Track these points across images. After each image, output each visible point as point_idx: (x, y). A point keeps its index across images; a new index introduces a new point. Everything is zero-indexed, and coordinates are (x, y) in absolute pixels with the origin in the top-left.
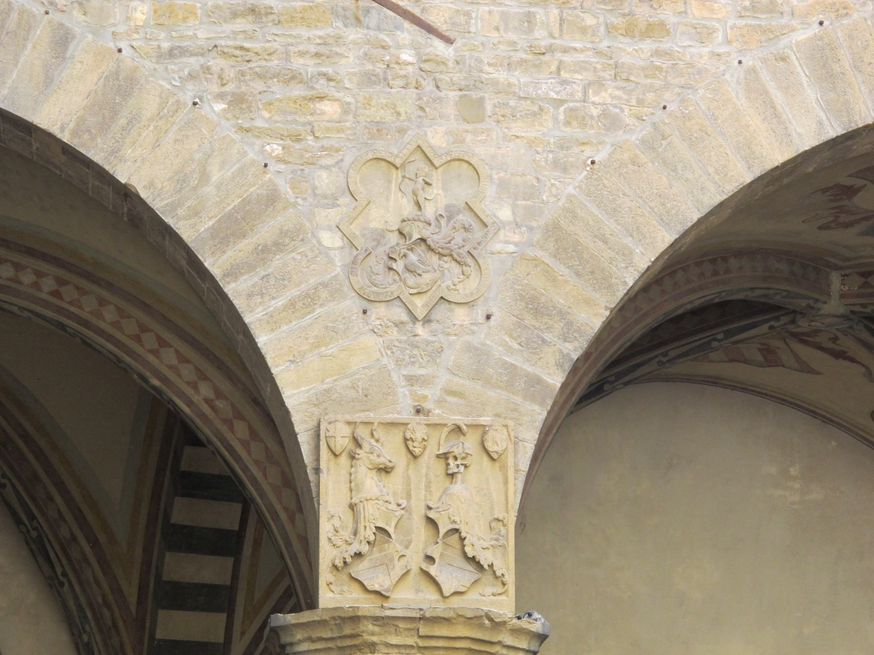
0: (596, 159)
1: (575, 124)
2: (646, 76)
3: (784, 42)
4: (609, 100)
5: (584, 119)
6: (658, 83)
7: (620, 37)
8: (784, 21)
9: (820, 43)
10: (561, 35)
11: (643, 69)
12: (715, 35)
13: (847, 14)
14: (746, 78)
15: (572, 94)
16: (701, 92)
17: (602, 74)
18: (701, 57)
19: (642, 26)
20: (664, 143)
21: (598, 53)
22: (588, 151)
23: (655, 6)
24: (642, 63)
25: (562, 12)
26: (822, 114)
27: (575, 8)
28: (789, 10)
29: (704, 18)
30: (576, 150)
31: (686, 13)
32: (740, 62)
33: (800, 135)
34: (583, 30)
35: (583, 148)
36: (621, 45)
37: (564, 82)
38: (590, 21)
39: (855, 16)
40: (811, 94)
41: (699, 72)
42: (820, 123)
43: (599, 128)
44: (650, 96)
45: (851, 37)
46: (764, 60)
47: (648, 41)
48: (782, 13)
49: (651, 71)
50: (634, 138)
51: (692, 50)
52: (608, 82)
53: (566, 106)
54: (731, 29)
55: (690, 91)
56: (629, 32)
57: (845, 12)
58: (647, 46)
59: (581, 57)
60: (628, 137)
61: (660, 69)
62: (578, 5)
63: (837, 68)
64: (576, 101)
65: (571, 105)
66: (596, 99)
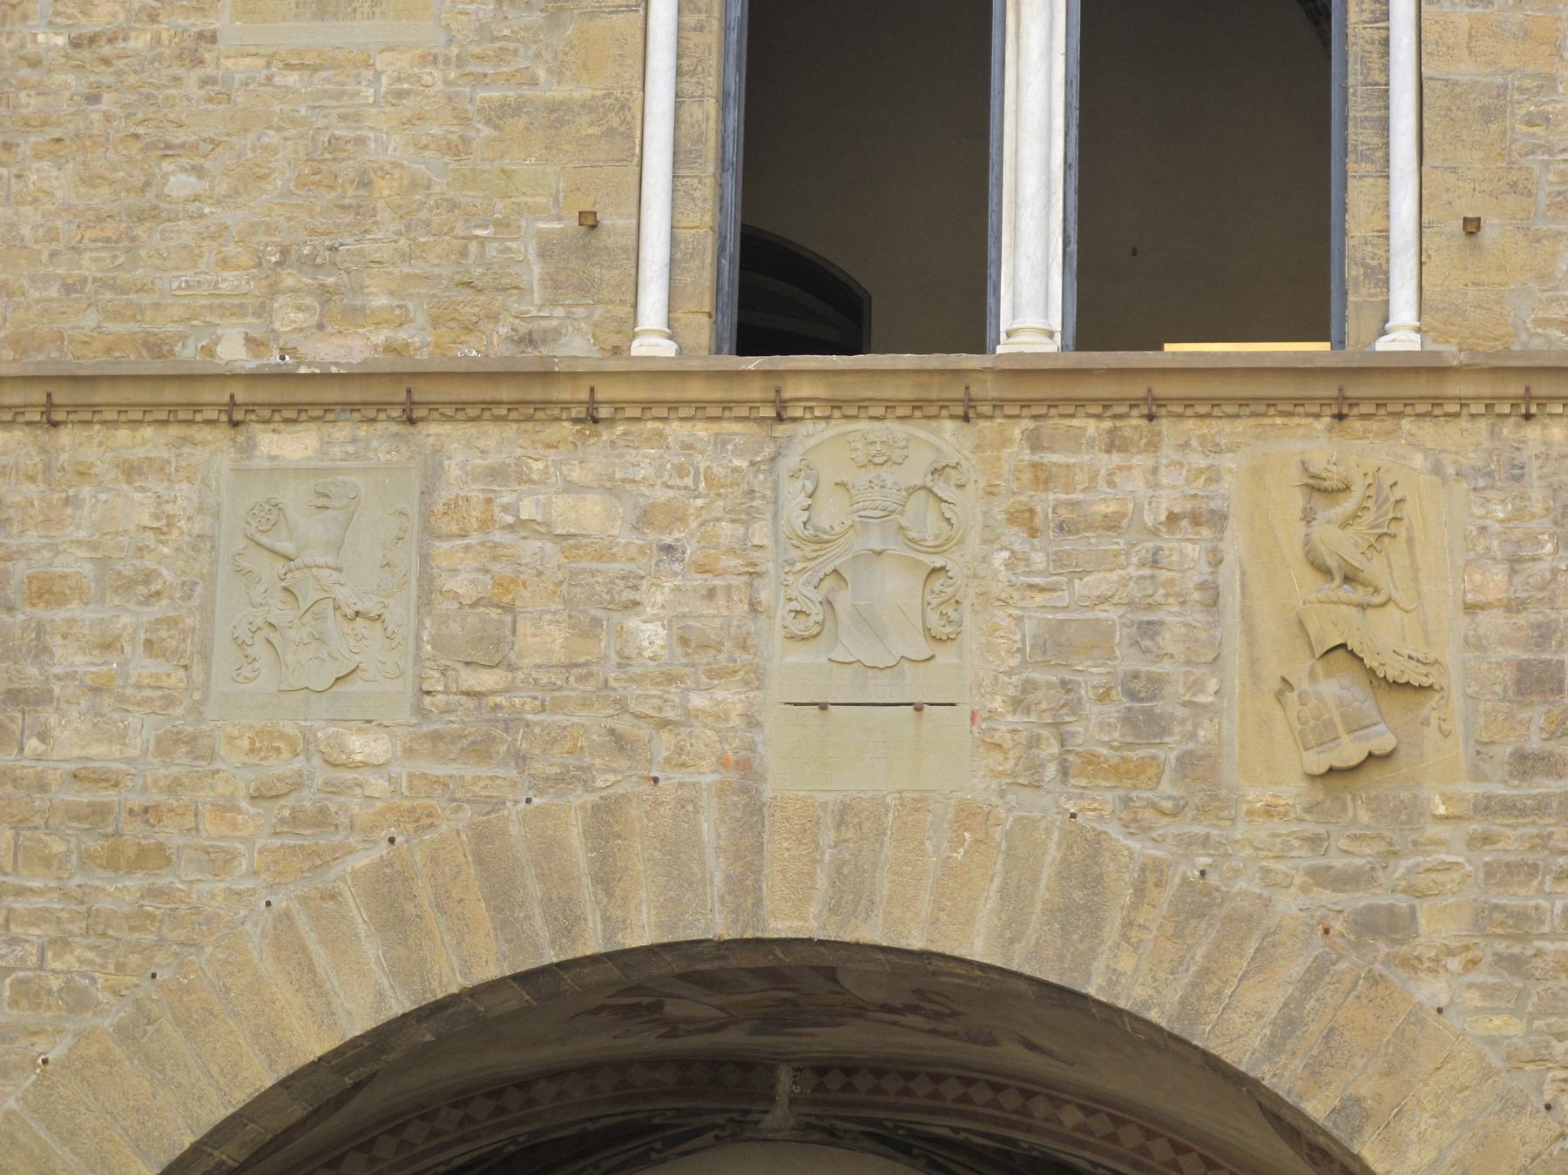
0: (50, 1057)
1: (24, 1003)
2: (132, 929)
3: (336, 870)
4: (76, 966)
5: (37, 995)
6: (149, 938)
7: (98, 871)
8: (337, 839)
9: (388, 871)
10: (15, 868)
11: (127, 917)
12: (236, 863)
13: (431, 825)
14: (275, 928)
15: (22, 959)
16: (209, 950)
17: (70, 927)
18: (213, 897)
19: (131, 852)
20: (151, 1029)
21: (65, 895)
22: (41, 1044)
23: (152, 821)
24: (126, 909)
25: (18, 834)
26: (384, 981)
27: (36, 828)
28: (347, 821)
29: (222, 838)
30: (24, 1042)
31: (197, 829)
32: (268, 904)
33: (349, 1013)
34: (47, 862)
35: (34, 1039)
36: (98, 883)
37: (14, 941)
38: (58, 847)
39: (444, 827)
40: (371, 950)
41: (208, 921)
42: (380, 994)
43: (60, 1009)
44: (134, 959)
45: (435, 860)
46: (304, 900)
47: (140, 874)
48: (336, 826)
49: (139, 920)
50: (106, 1023)
51: (201, 886)
52: (77, 939)
53: (14, 976)
54: (260, 853)
55: (192, 950)
56: (113, 862)
57: (429, 821)
58: (135, 882)
59: (40, 902)
60: (99, 1021)
61: (152, 917)
62: (42, 822)
63: (410, 908)
64: (28, 969)
65: (21, 974)
66: (57, 965)
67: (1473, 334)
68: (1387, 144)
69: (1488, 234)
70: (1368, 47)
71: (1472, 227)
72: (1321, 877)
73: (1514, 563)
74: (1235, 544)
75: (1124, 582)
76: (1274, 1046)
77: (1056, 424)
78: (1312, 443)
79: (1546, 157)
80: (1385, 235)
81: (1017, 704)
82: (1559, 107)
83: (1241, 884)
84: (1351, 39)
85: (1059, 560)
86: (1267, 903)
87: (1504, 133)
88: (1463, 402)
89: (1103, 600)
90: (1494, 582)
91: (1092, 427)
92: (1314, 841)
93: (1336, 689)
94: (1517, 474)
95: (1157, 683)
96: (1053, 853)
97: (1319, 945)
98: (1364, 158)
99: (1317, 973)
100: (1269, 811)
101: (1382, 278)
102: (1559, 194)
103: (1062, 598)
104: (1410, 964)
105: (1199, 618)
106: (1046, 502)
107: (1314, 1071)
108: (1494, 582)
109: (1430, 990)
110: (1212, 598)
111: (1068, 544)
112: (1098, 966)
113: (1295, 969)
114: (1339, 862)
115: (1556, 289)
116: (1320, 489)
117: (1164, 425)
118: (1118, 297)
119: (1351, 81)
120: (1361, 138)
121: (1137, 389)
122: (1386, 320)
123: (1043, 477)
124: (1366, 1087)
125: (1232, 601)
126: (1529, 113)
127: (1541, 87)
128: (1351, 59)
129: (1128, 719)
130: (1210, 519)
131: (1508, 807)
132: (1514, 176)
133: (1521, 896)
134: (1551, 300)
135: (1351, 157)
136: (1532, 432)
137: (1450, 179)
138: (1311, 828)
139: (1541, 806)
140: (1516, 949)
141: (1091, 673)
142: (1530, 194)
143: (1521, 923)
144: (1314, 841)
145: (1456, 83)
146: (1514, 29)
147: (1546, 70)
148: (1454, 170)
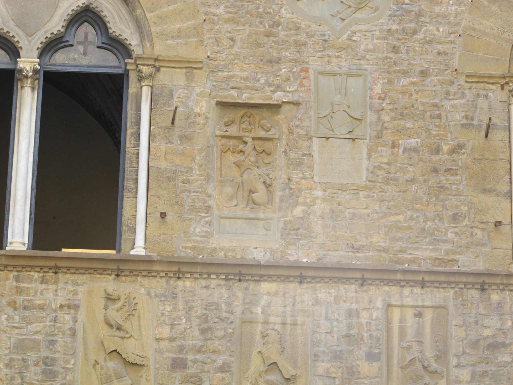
67: (162, 250)
68: (137, 187)
69: (168, 218)
70: (132, 155)
71: (163, 215)
73: (172, 325)
74: (81, 316)
75: (45, 327)
77: (24, 274)
78: (108, 284)
79: (188, 194)
80: (135, 217)
81: (7, 366)
82: (193, 178)
84: (127, 152)
85: (24, 319)
87: (175, 185)
88: (158, 272)
89: (38, 332)
90: (166, 331)
91: (36, 275)
93: (112, 364)
94: (175, 296)
95: (54, 361)
98: (129, 191)
101: (133, 230)
102: (192, 206)
103: (24, 331)
105: (69, 339)
106: (20, 299)
108: (166, 331)
110: (73, 333)
111: (27, 313)
115: (189, 237)
116: (110, 299)
117: (60, 276)
118: (47, 232)
119: (126, 166)
120: (129, 185)
121: (52, 263)
122: (134, 245)
123: (19, 291)
125: (80, 335)
126: (183, 179)
127: (188, 171)
128: (126, 159)
129: (44, 372)
130: (73, 307)
132: (178, 199)
134: (188, 240)
135: (125, 191)
136: (180, 283)
137: (157, 200)
141: (32, 356)
142: (182, 206)
145: (160, 168)
146: (180, 152)
147: (189, 165)
148: (158, 197)
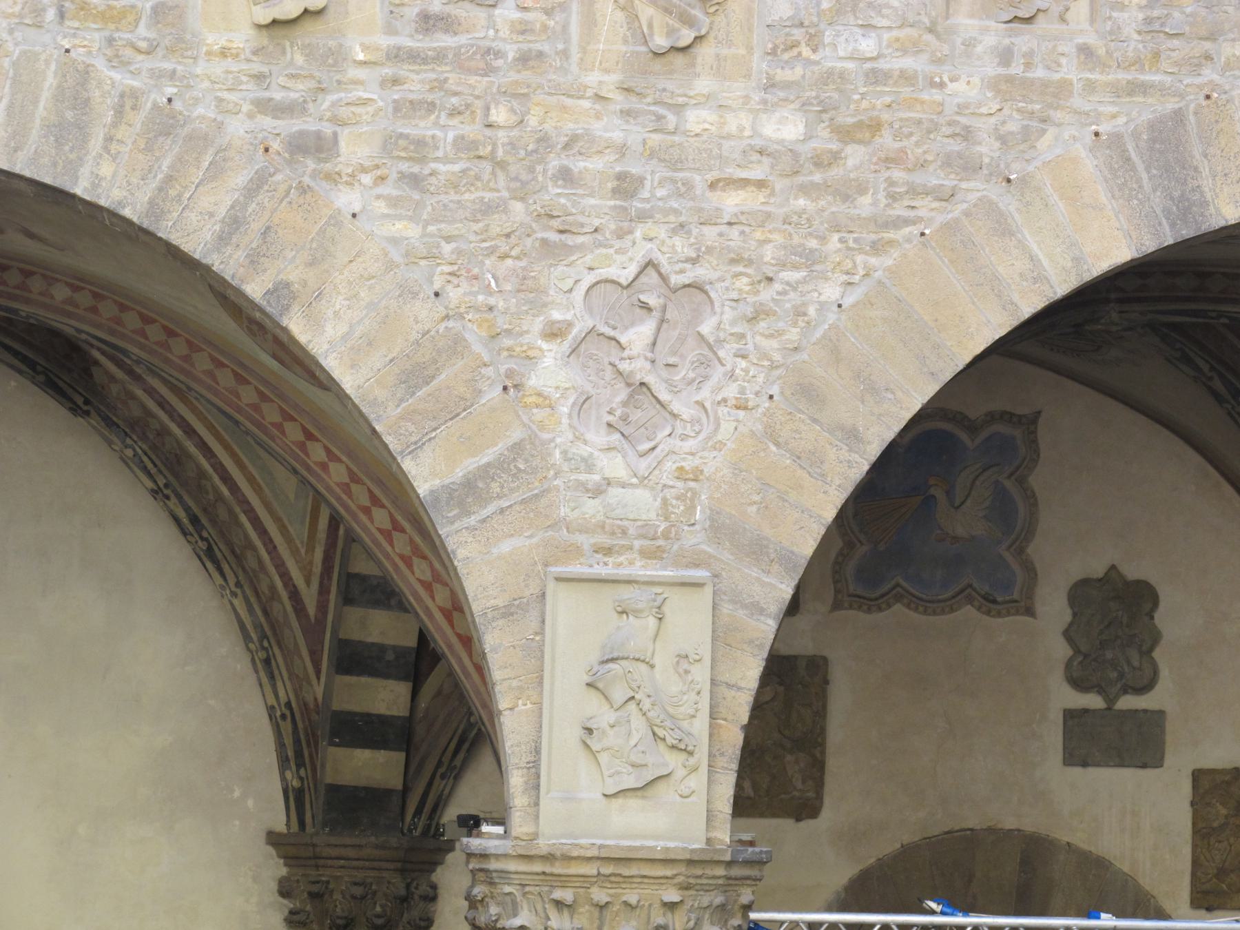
72: (264, 106)
76: (222, 239)
83: (200, 111)
86: (220, 126)
92: (259, 78)
96: (50, 80)
97: (260, 160)
99: (259, 182)
100: (224, 53)
104: (333, 178)
107: (254, 260)
109: (347, 199)
112: (85, 171)
113: (240, 179)
114: (278, 95)
124: (293, 274)
131: (414, 57)
133: (422, 127)
138: (257, 67)
139: (440, 57)
140: (416, 169)
143: (420, 148)
144: (259, 78)
